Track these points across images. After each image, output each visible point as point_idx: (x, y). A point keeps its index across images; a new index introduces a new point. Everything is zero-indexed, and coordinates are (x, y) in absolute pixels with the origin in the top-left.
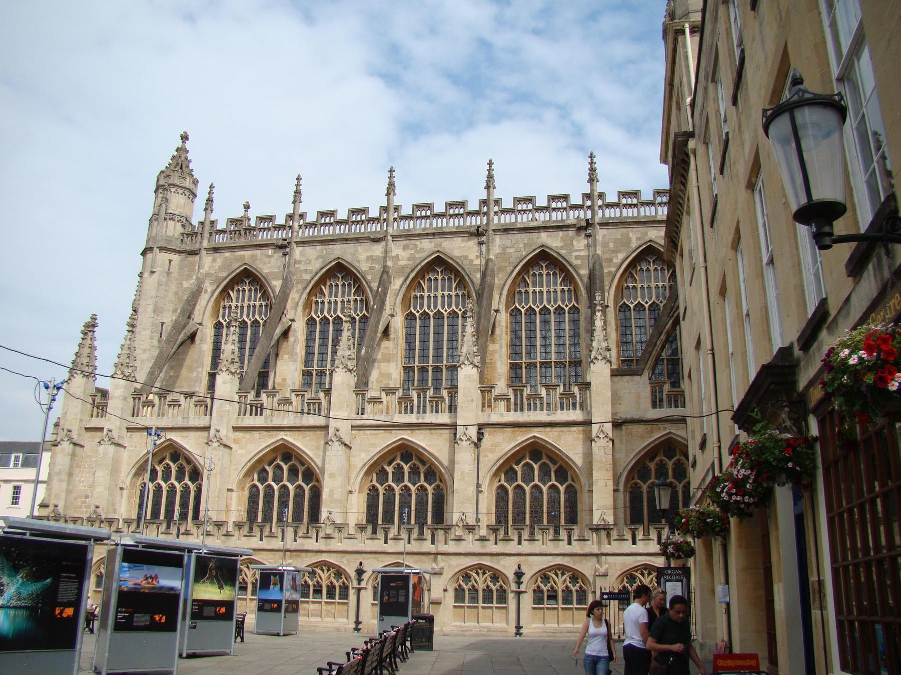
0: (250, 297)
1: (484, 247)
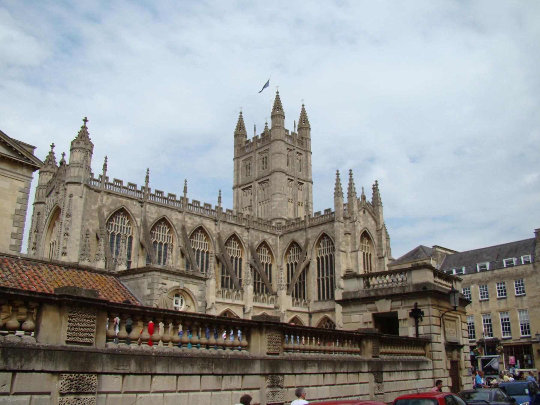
0: (122, 222)
1: (217, 227)
